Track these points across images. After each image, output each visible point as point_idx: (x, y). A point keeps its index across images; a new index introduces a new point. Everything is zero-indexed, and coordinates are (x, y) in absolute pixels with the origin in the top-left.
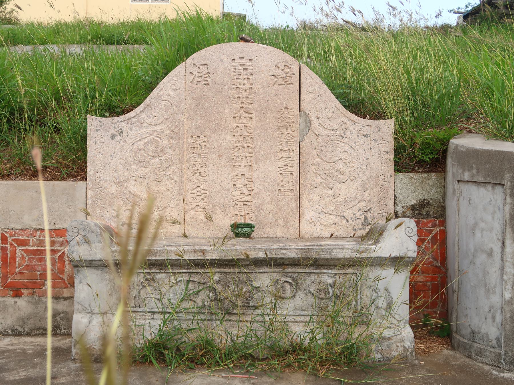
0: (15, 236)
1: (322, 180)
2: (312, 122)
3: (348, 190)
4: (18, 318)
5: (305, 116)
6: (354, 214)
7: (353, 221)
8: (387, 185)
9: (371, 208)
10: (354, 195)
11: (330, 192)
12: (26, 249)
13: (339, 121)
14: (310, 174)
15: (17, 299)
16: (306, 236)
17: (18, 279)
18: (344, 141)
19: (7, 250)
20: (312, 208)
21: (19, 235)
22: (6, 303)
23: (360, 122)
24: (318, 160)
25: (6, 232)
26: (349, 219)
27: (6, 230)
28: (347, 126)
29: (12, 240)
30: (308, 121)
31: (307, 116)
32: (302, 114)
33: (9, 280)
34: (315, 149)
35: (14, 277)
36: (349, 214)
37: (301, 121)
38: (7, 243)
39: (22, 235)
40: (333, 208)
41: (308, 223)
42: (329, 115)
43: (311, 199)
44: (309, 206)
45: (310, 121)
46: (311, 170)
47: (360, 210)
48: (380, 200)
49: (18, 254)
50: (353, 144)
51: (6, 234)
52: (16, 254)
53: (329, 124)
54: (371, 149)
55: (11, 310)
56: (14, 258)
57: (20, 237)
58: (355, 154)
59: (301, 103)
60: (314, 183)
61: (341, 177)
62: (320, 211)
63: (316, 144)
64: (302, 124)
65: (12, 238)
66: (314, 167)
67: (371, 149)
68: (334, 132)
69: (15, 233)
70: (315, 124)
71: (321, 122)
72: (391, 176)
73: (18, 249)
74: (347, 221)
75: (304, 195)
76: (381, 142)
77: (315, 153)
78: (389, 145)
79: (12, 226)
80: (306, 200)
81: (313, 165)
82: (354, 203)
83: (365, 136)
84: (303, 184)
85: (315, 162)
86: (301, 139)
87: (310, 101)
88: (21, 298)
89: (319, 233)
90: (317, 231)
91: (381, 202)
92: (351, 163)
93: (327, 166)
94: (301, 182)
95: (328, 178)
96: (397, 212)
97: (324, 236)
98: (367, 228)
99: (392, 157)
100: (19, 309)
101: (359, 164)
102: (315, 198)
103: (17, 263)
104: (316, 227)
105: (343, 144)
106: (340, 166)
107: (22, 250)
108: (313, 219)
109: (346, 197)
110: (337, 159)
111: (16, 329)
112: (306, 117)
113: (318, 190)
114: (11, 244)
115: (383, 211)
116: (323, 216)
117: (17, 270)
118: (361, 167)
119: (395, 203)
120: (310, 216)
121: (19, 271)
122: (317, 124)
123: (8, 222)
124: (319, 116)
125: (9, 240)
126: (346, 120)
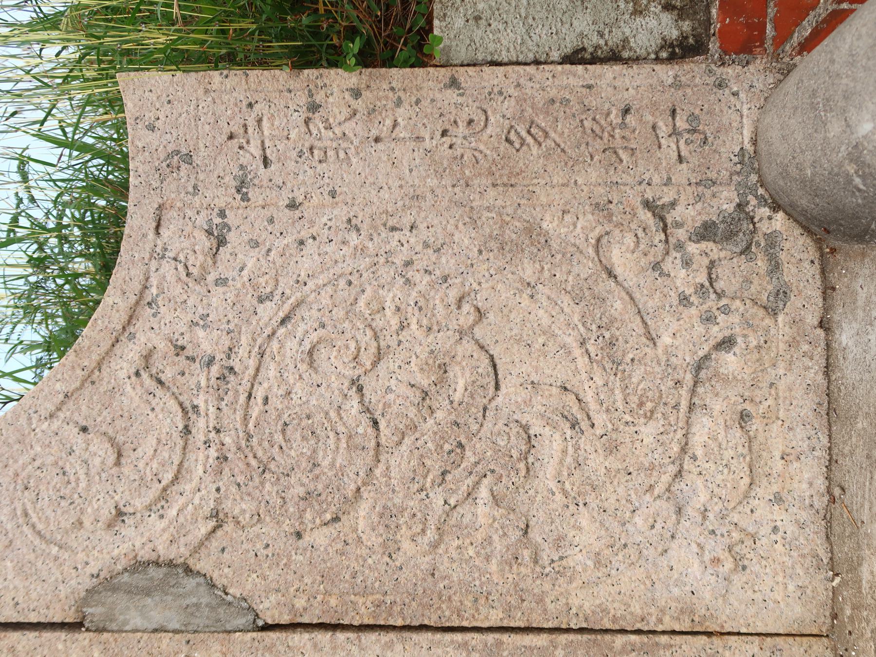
1: (483, 493)
2: (145, 554)
3: (539, 341)
5: (110, 598)
6: (684, 300)
7: (726, 310)
8: (509, 107)
9: (647, 205)
10: (566, 301)
11: (552, 445)
13: (132, 395)
14: (444, 566)
16: (823, 595)
18: (252, 363)
20: (650, 553)
23: (137, 273)
24: (363, 515)
26: (717, 333)
28: (162, 346)
30: (139, 580)
31: (106, 584)
32: (95, 612)
34: (299, 535)
36: (681, 336)
37: (137, 621)
40: (649, 431)
41: (738, 579)
42: (102, 452)
43: (598, 563)
44: (640, 573)
45: (138, 566)
46: (425, 562)
47: (656, 266)
48: (599, 145)
50: (266, 311)
53: (151, 454)
54: (293, 205)
58: (325, 301)
59: (33, 618)
60: (498, 545)
61: (460, 380)
62: (666, 508)
63: (269, 529)
64: (157, 617)
66: (406, 545)
67: (293, 205)
68: (200, 425)
70: (149, 536)
71: (139, 504)
72: (454, 83)
74: (727, 343)
75: (575, 602)
76: (254, 148)
77: (320, 537)
78: (273, 96)
80: (604, 592)
81: (390, 550)
82: (618, 305)
83: (221, 242)
84: (508, 610)
85: (372, 539)
86: (241, 621)
87: (20, 569)
89: (803, 516)
90: (791, 529)
91: (608, 139)
92: (378, 323)
93: (399, 462)
94: (495, 618)
95: (471, 456)
96: (666, 44)
97: (821, 483)
98: (764, 227)
99: (337, 82)
101: (386, 273)
102: (587, 533)
104: (766, 530)
105: (271, 371)
106: (394, 386)
108: (715, 547)
109: (577, 352)
110: (353, 405)
112: (115, 589)
113: (538, 518)
115: (663, 129)
116: (698, 492)
118: (399, 261)
119: (614, 57)
120: (696, 569)
122: (155, 524)
124: (107, 512)
126: (130, 354)
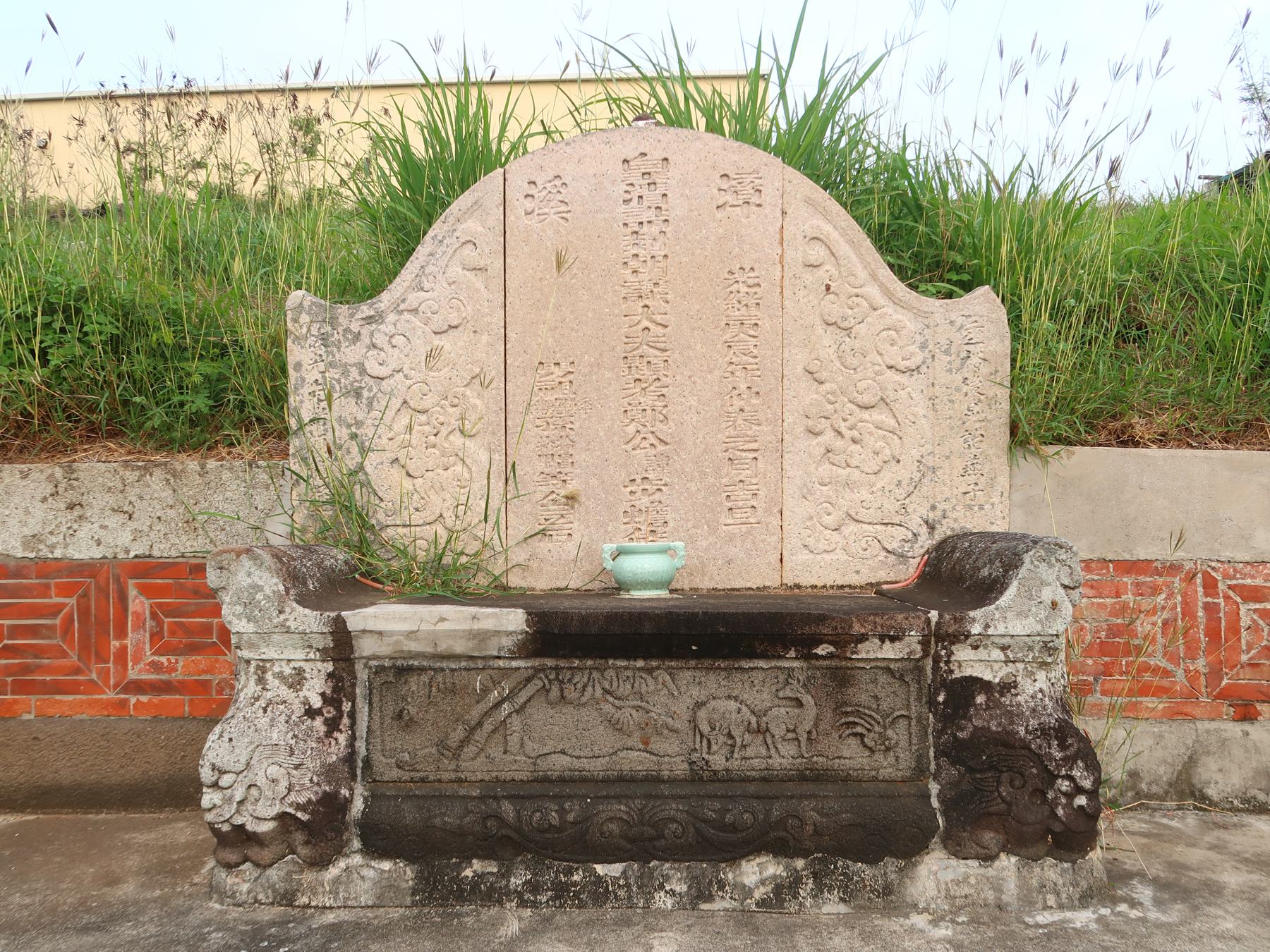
0: (1234, 578)
4: (1257, 772)
12: (1264, 610)
15: (1247, 726)
17: (1246, 678)
19: (1219, 612)
21: (1244, 577)
22: (1224, 735)
25: (1213, 568)
27: (1213, 564)
29: (1230, 587)
33: (1225, 682)
35: (1238, 674)
38: (1216, 595)
39: (1253, 577)
49: (1245, 621)
51: (1213, 574)
52: (1239, 619)
55: (1237, 751)
56: (1235, 629)
57: (1249, 581)
65: (1229, 582)
69: (1235, 570)
73: (1243, 609)
79: (1226, 554)
88: (1257, 724)
100: (1257, 749)
103: (1243, 641)
107: (1255, 611)
111: (1255, 798)
114: (1227, 598)
117: (1244, 658)
121: (1250, 659)
123: (1217, 545)
125: (1221, 586)
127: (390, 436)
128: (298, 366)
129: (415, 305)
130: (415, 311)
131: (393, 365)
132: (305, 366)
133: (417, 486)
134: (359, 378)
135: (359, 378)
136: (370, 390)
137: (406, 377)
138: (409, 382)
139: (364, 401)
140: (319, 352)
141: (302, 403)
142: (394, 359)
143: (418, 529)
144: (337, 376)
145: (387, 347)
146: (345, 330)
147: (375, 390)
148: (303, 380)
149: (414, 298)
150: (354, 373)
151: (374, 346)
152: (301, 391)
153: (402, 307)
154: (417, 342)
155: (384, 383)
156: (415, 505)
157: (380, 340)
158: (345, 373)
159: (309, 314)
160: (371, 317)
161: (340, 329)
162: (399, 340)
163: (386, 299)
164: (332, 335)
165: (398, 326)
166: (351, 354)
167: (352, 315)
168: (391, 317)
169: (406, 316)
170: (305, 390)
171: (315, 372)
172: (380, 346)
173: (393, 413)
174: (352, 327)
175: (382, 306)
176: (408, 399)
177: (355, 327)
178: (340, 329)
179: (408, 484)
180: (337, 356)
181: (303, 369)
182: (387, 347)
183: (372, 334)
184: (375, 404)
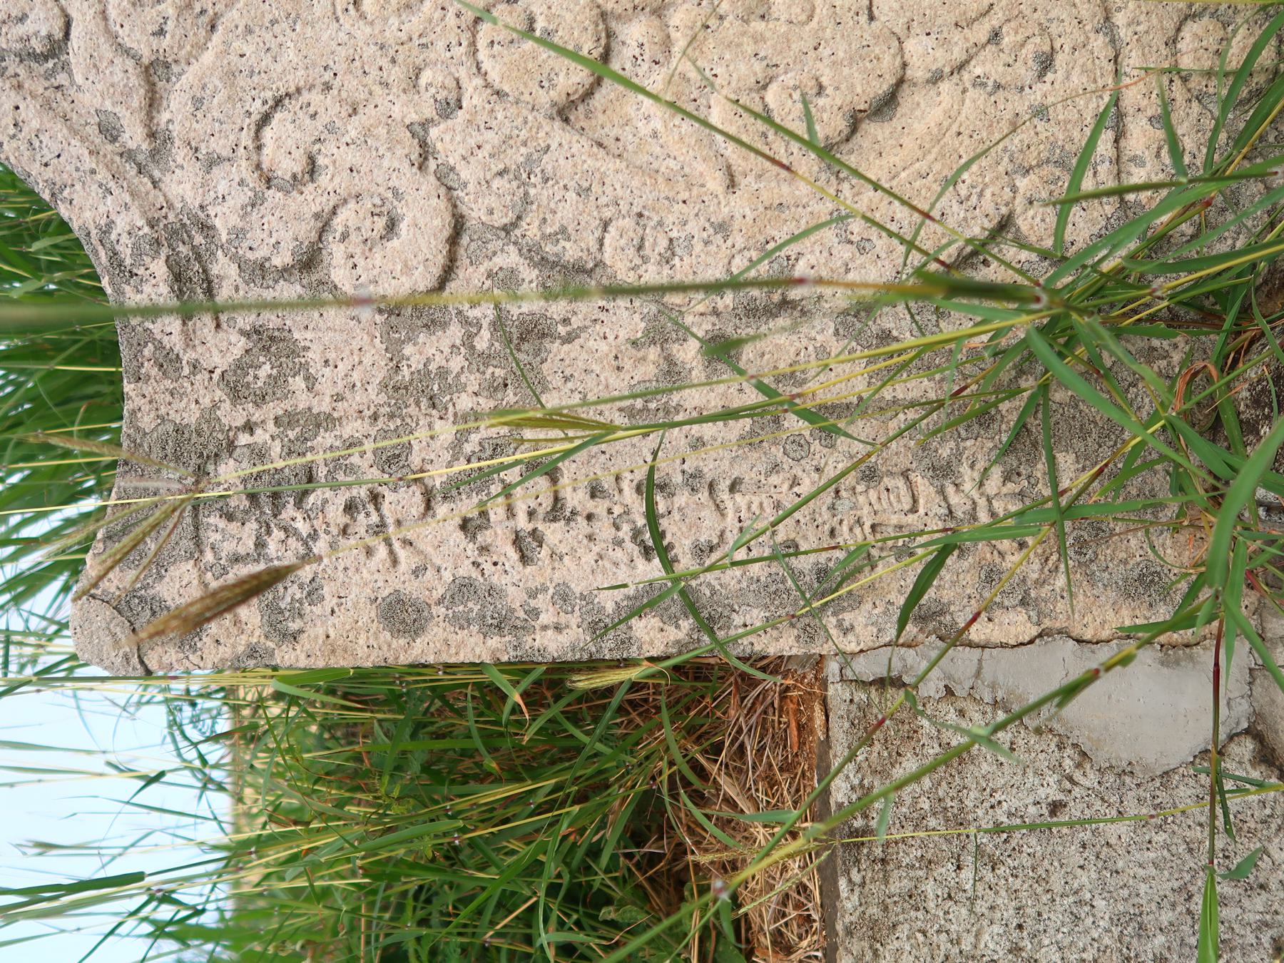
127: (715, 183)
128: (401, 614)
129: (123, 74)
130: (155, 74)
131: (394, 166)
132: (402, 582)
133: (942, 59)
134: (455, 332)
135: (455, 332)
136: (508, 280)
137: (449, 107)
138: (474, 97)
139: (558, 309)
140: (336, 515)
141: (571, 590)
142: (366, 162)
143: (1133, 60)
144: (446, 431)
145: (312, 200)
146: (237, 393)
147: (510, 258)
148: (463, 588)
149: (99, 82)
150: (432, 350)
151: (309, 261)
152: (515, 598)
153: (134, 136)
154: (288, 67)
155: (476, 212)
156: (1026, 72)
157: (279, 231)
158: (429, 391)
159: (159, 566)
160: (178, 277)
161: (232, 416)
162: (283, 145)
163: (95, 207)
164: (259, 454)
165: (220, 146)
166: (342, 356)
167: (168, 362)
168: (182, 186)
169: (174, 112)
170: (512, 579)
171: (425, 534)
172: (306, 230)
173: (609, 165)
174: (221, 362)
175: (128, 223)
176: (544, 98)
177: (222, 347)
178: (232, 416)
179: (924, 113)
180: (352, 428)
181: (413, 588)
182: (312, 200)
183: (259, 271)
184: (571, 252)
